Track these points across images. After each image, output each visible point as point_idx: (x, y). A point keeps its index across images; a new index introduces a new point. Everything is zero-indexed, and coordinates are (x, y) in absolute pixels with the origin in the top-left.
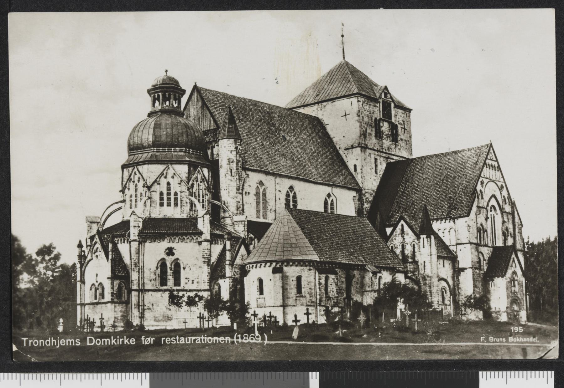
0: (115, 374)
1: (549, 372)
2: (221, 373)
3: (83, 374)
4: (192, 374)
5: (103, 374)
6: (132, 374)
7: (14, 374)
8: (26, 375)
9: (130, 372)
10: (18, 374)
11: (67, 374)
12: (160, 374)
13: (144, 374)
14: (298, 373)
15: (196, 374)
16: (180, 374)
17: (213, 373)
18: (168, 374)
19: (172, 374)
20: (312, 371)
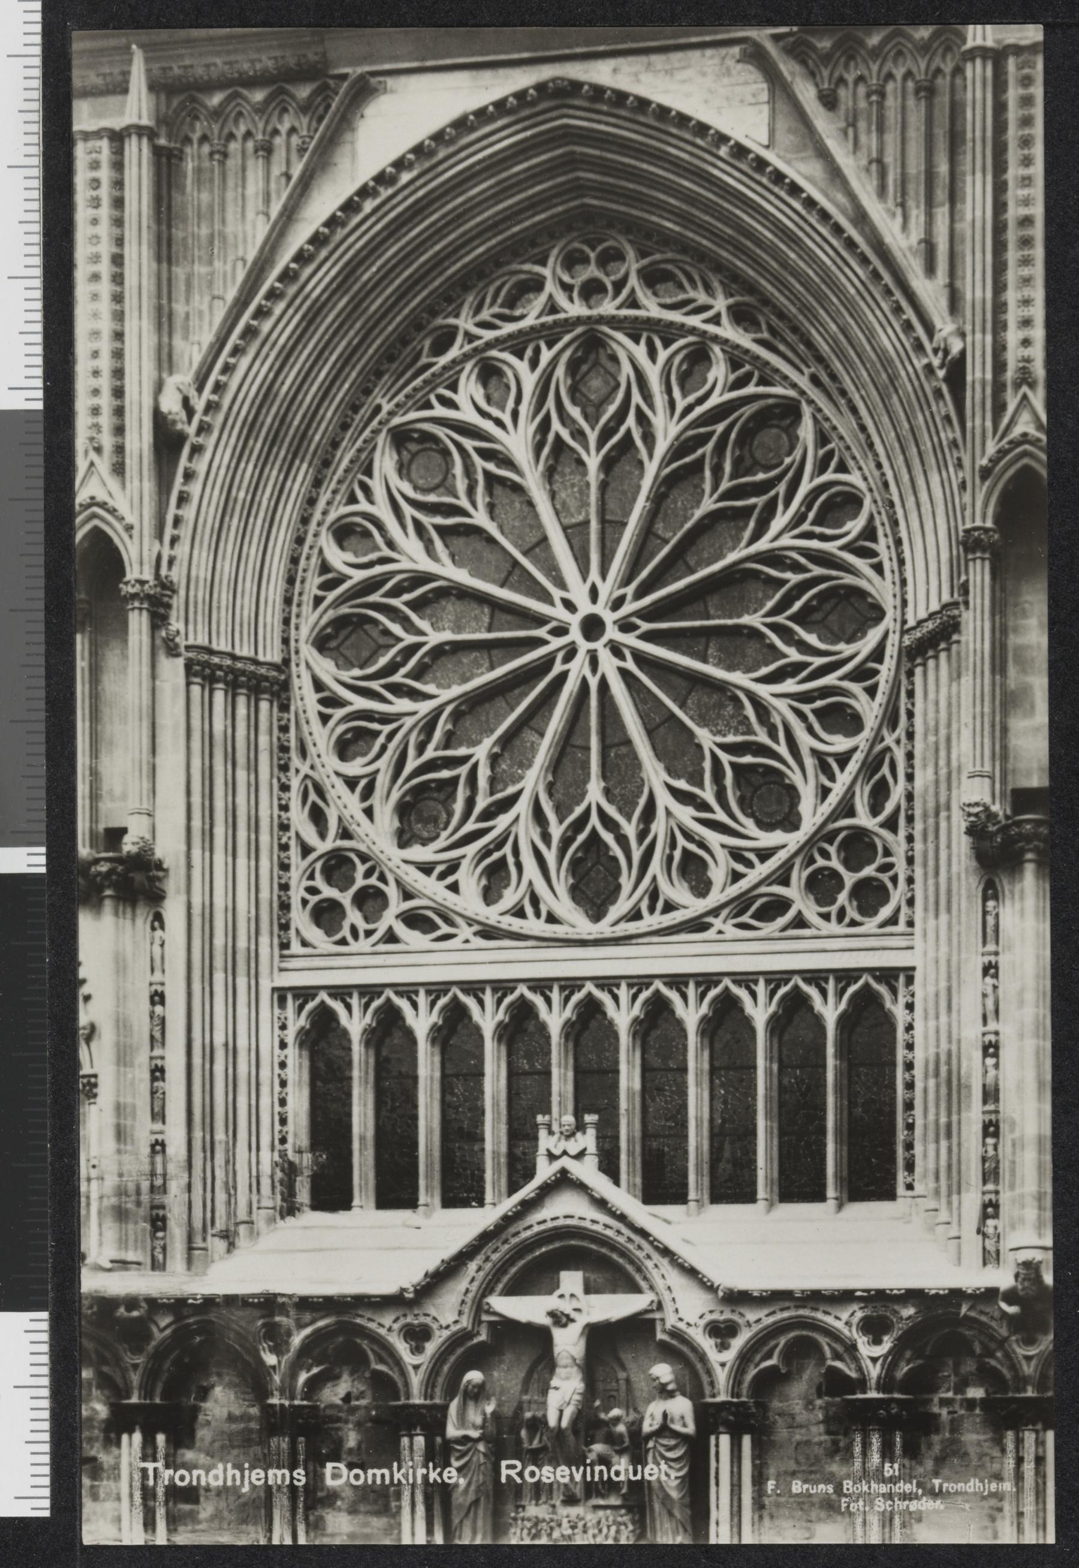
0: (39, 316)
2: (41, 605)
3: (37, 228)
4: (41, 527)
5: (38, 283)
6: (39, 361)
8: (37, 73)
10: (38, 50)
11: (37, 183)
12: (40, 438)
13: (40, 394)
14: (43, 816)
15: (41, 538)
16: (41, 494)
17: (41, 582)
18: (41, 461)
19: (41, 472)
20: (48, 855)
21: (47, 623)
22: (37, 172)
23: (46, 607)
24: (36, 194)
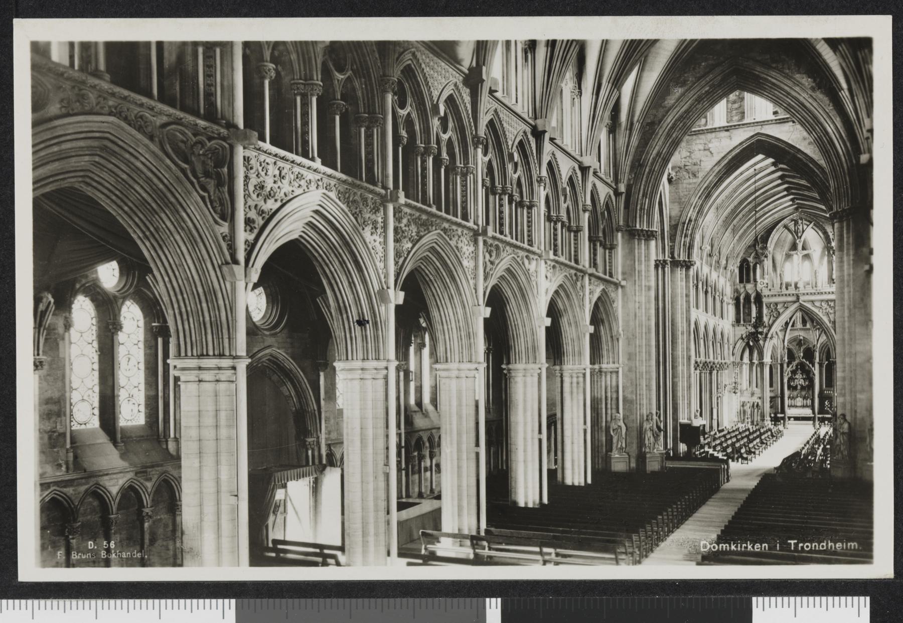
0: (182, 601)
1: (862, 598)
2: (347, 600)
3: (131, 601)
4: (303, 600)
5: (163, 601)
6: (207, 601)
7: (23, 601)
8: (42, 602)
9: (204, 598)
10: (30, 602)
11: (106, 602)
12: (252, 601)
13: (227, 601)
14: (468, 600)
15: (309, 600)
16: (284, 600)
17: (335, 600)
18: (265, 601)
19: (271, 600)
21: (357, 597)
22: (99, 602)
23: (349, 598)
24: (112, 601)
